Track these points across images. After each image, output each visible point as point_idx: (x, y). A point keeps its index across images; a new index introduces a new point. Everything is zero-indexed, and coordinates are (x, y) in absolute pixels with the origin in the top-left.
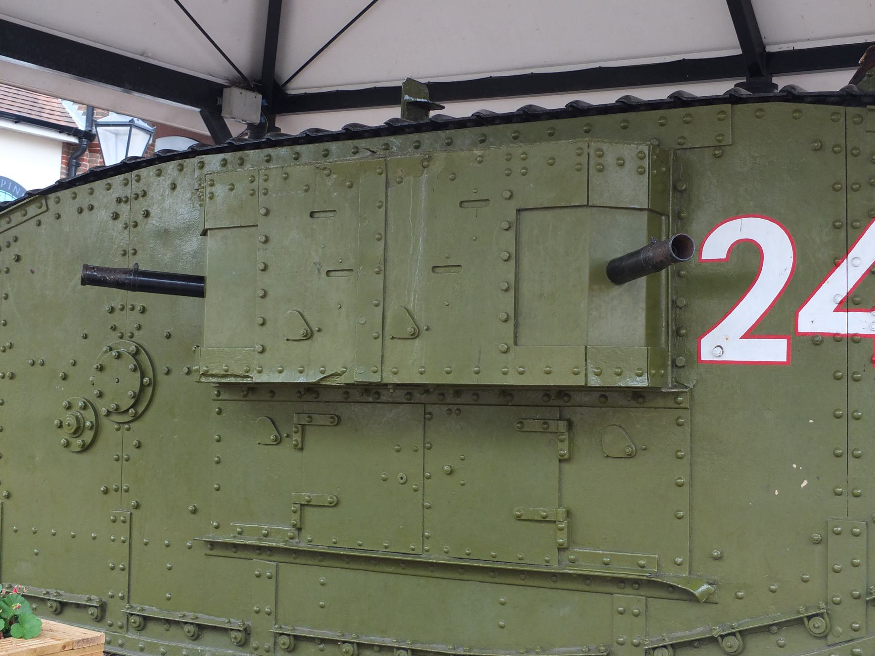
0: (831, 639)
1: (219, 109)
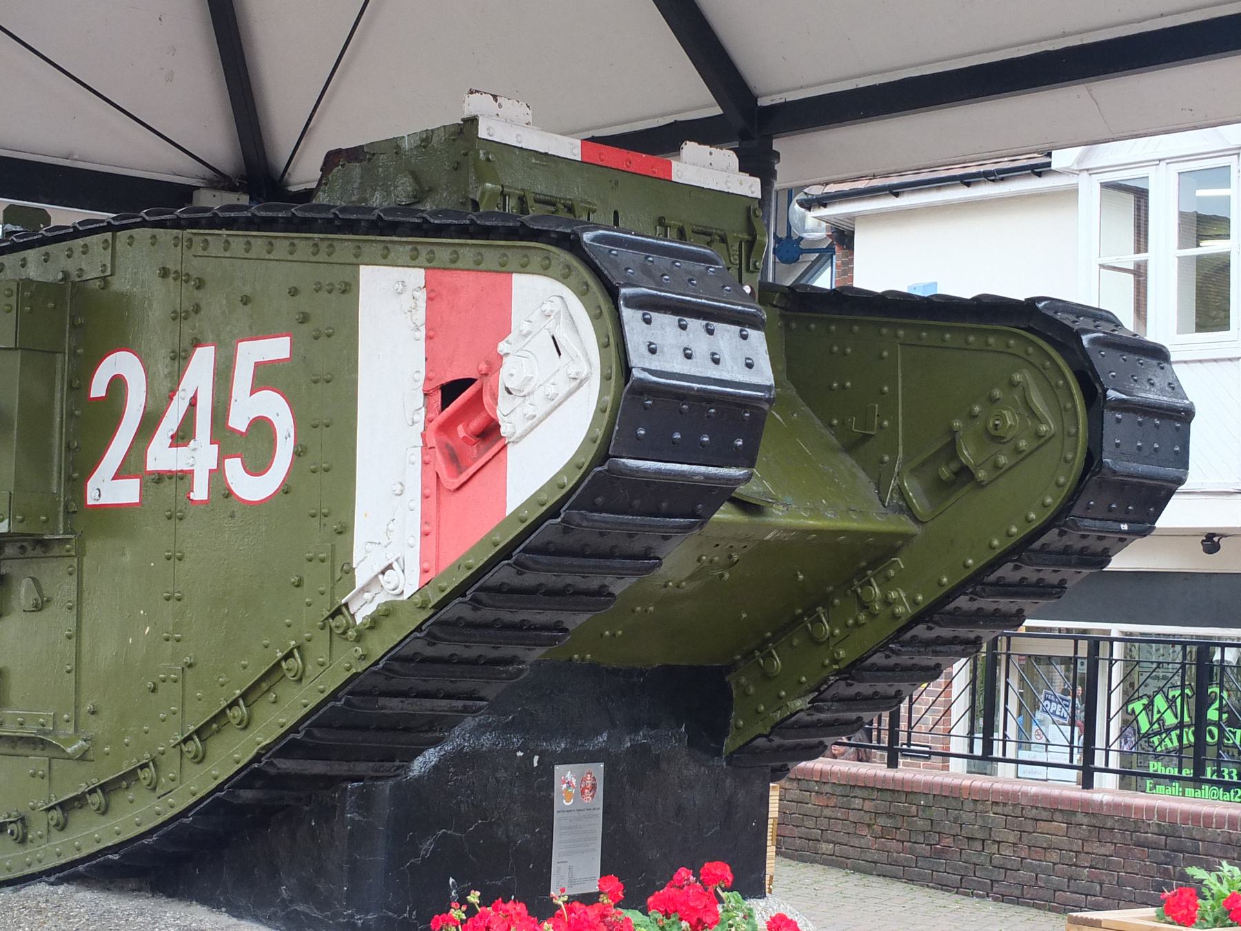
0: (159, 791)
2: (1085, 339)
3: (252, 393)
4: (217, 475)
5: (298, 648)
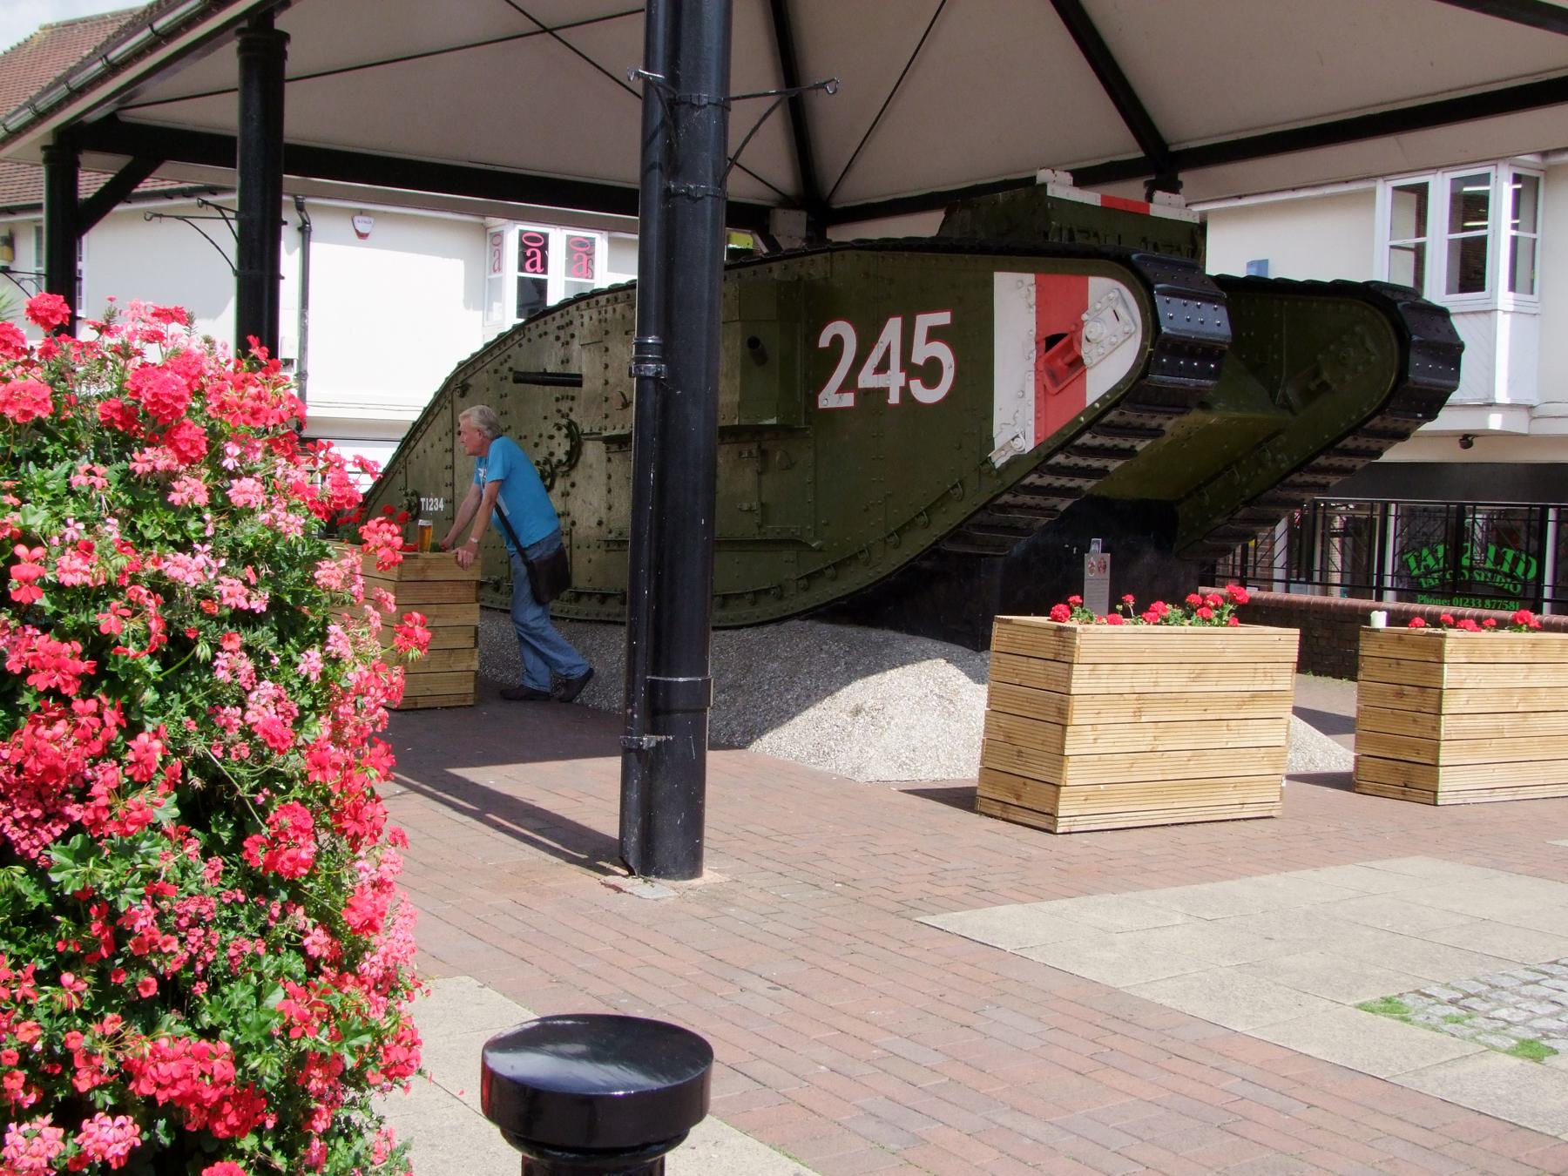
0: (871, 566)
1: (768, 227)
2: (1399, 305)
3: (927, 343)
4: (905, 391)
5: (960, 482)
